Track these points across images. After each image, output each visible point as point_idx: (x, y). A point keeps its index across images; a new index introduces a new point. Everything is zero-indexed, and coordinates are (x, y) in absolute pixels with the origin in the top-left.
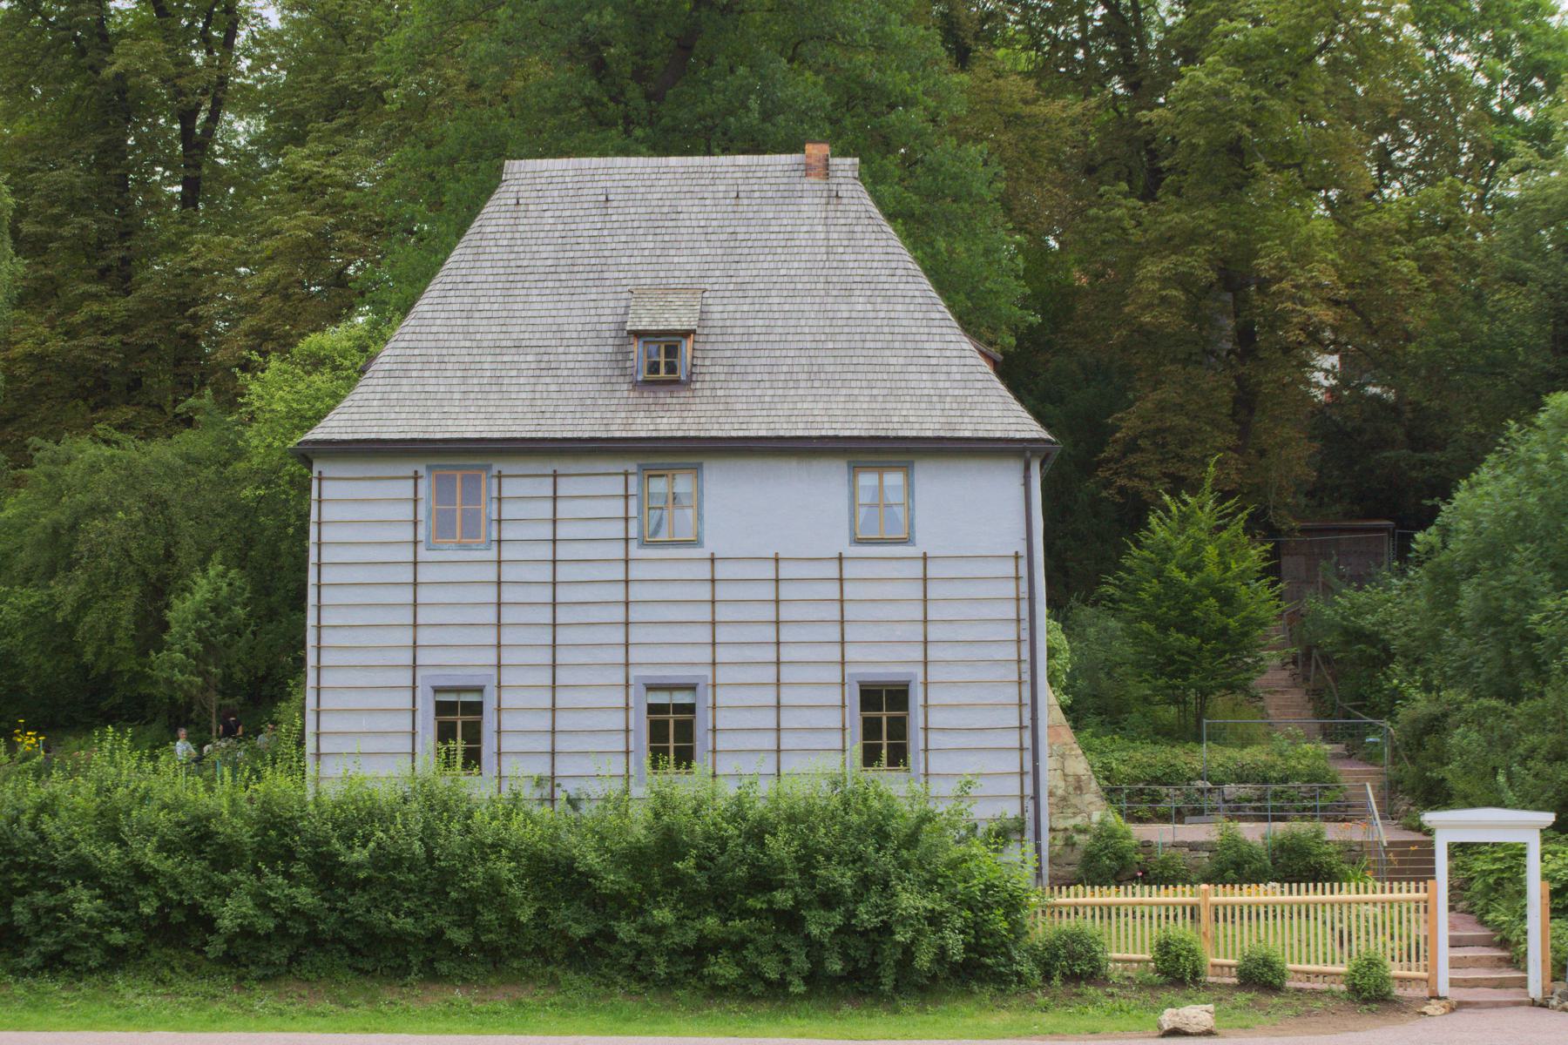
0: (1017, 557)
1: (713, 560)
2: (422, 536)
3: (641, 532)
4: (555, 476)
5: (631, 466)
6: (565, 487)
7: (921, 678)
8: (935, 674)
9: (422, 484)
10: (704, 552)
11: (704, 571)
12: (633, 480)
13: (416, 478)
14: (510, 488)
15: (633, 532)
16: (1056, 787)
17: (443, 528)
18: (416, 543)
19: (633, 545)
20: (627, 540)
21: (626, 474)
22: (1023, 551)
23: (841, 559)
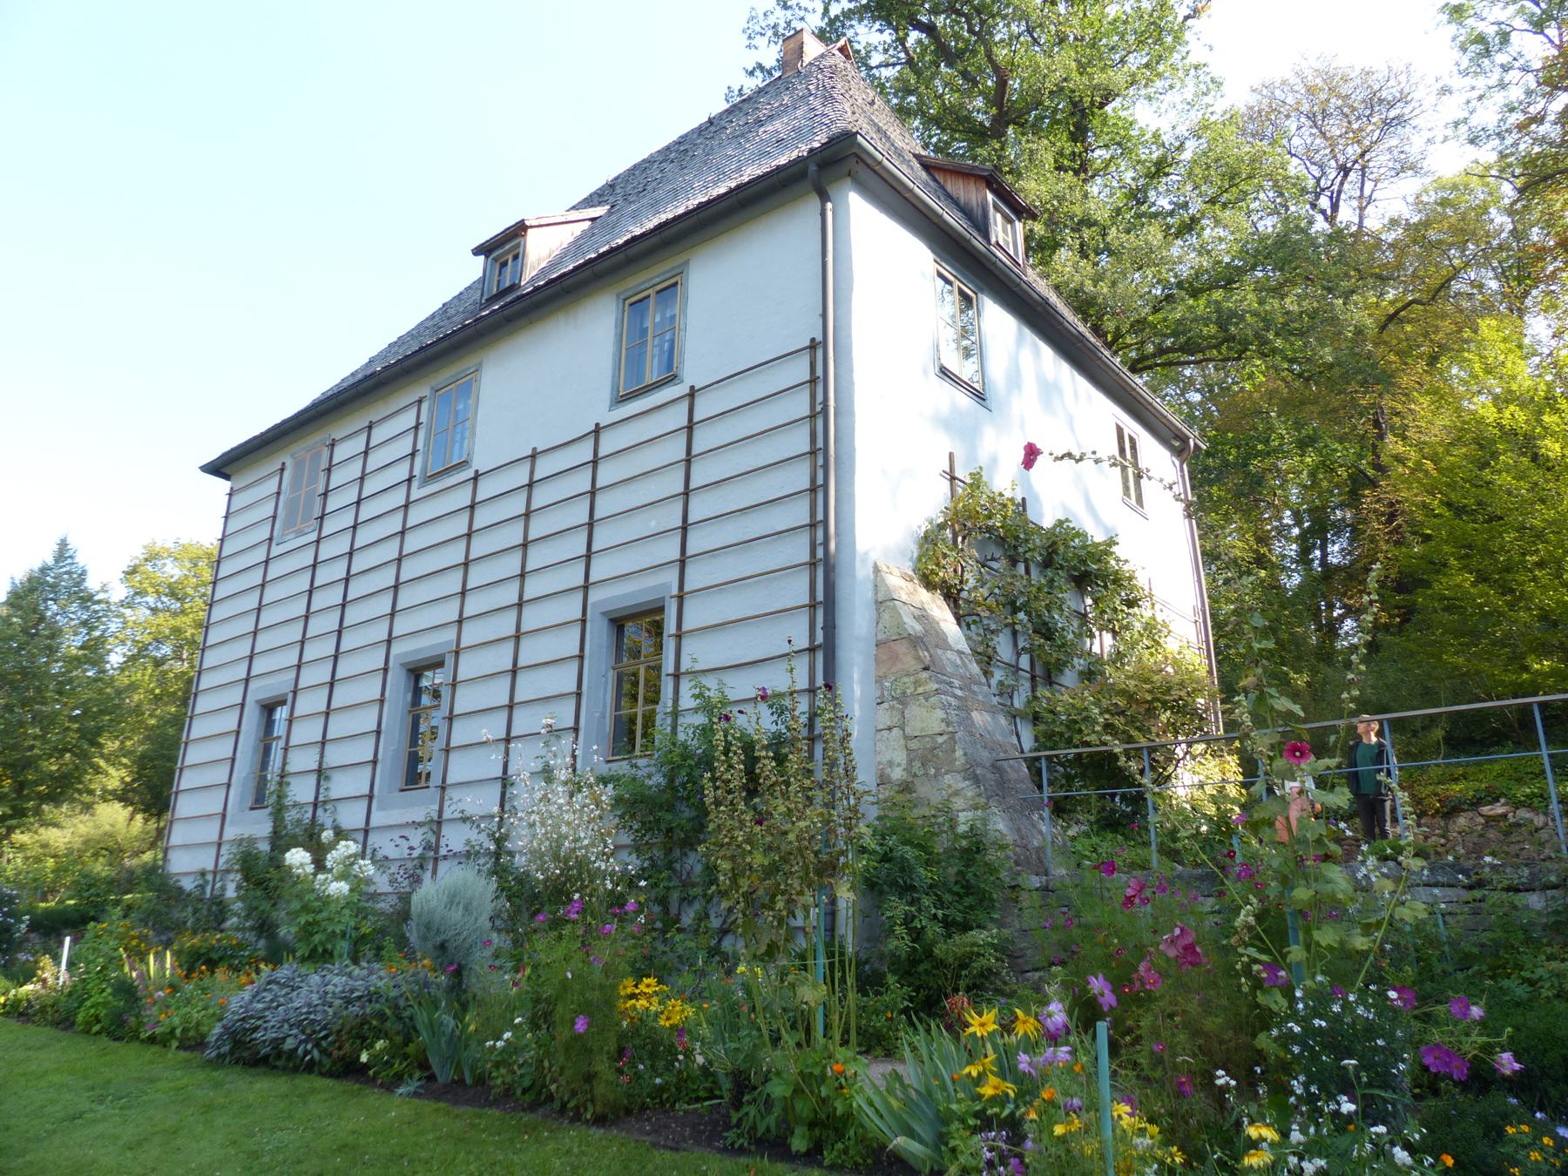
0: (813, 346)
1: (476, 478)
2: (275, 533)
3: (425, 468)
4: (370, 427)
5: (423, 390)
6: (379, 435)
7: (675, 591)
8: (695, 578)
9: (286, 474)
10: (470, 473)
11: (462, 498)
12: (425, 406)
13: (282, 470)
14: (341, 453)
15: (417, 472)
16: (891, 763)
17: (289, 523)
18: (271, 539)
19: (415, 484)
20: (409, 480)
21: (420, 401)
22: (819, 338)
23: (597, 430)
